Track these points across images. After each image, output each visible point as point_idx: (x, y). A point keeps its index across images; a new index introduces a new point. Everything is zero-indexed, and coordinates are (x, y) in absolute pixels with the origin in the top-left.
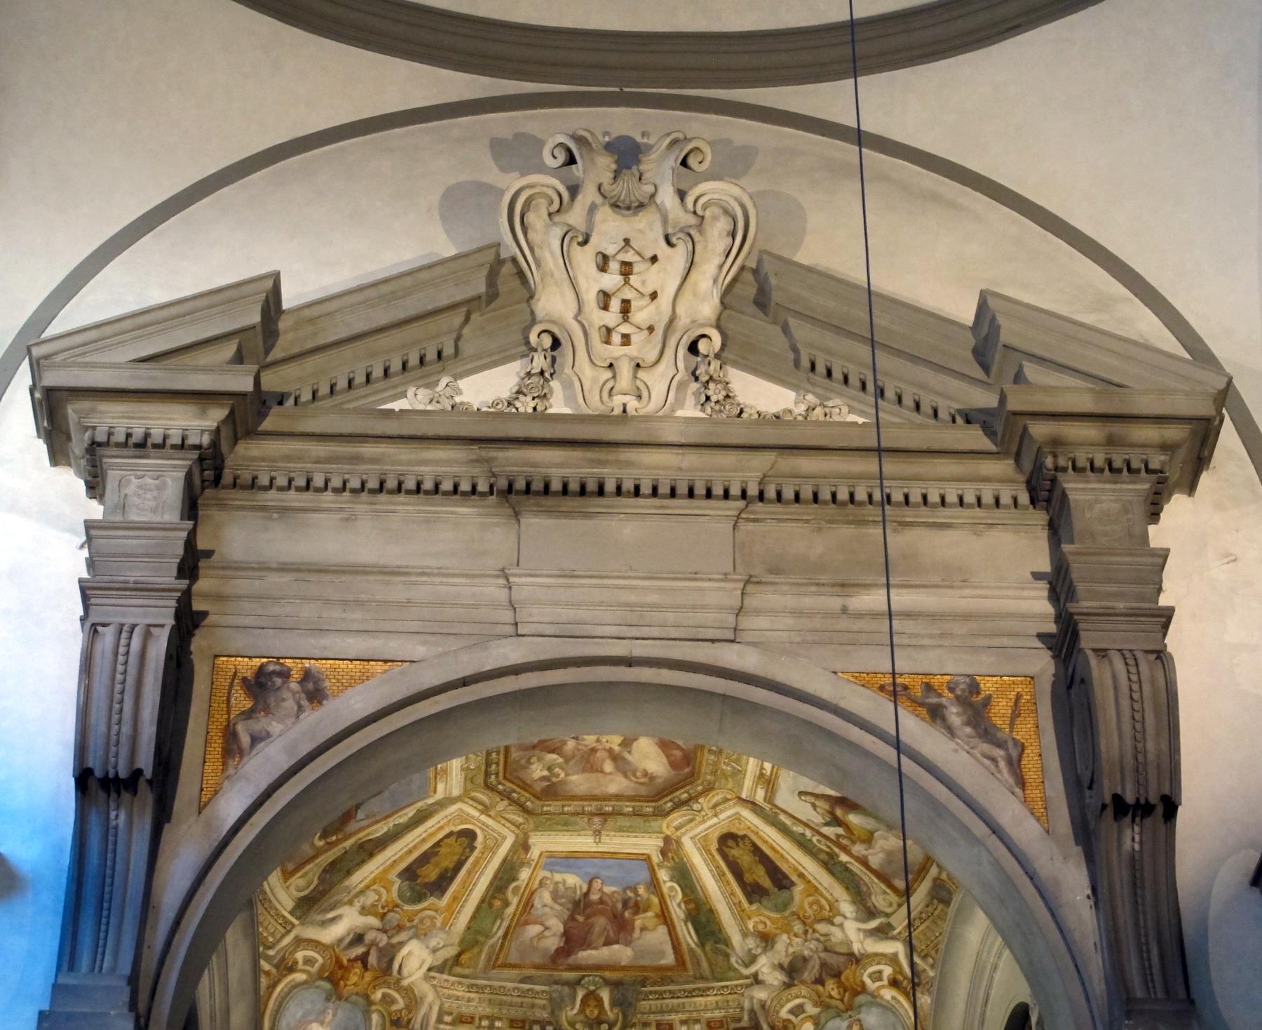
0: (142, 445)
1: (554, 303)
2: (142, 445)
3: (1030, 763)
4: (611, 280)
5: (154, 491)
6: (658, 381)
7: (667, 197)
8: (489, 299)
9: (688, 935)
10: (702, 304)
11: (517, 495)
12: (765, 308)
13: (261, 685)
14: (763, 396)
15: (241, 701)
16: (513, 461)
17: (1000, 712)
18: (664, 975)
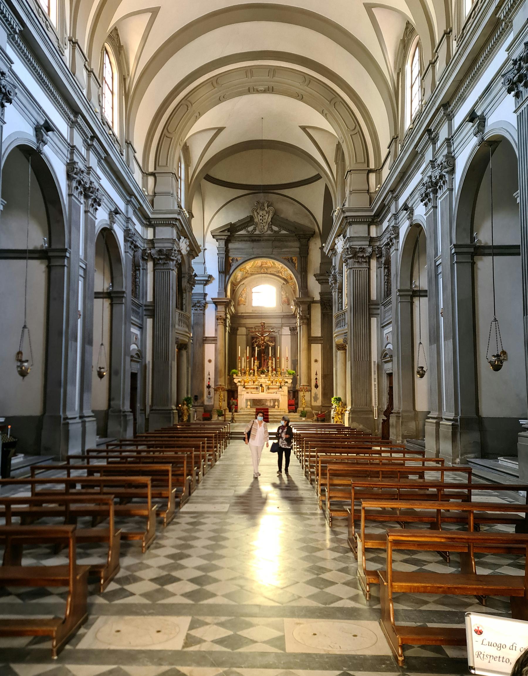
0: (221, 239)
1: (256, 220)
2: (221, 239)
3: (296, 265)
4: (261, 218)
5: (223, 243)
6: (266, 228)
7: (266, 209)
8: (250, 221)
9: (272, 264)
10: (270, 220)
11: (253, 241)
12: (276, 219)
13: (232, 260)
14: (275, 228)
15: (231, 261)
16: (253, 238)
17: (294, 260)
18: (270, 267)
